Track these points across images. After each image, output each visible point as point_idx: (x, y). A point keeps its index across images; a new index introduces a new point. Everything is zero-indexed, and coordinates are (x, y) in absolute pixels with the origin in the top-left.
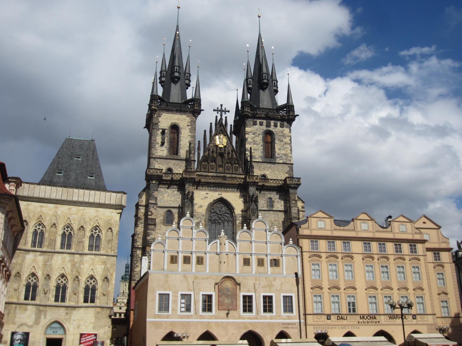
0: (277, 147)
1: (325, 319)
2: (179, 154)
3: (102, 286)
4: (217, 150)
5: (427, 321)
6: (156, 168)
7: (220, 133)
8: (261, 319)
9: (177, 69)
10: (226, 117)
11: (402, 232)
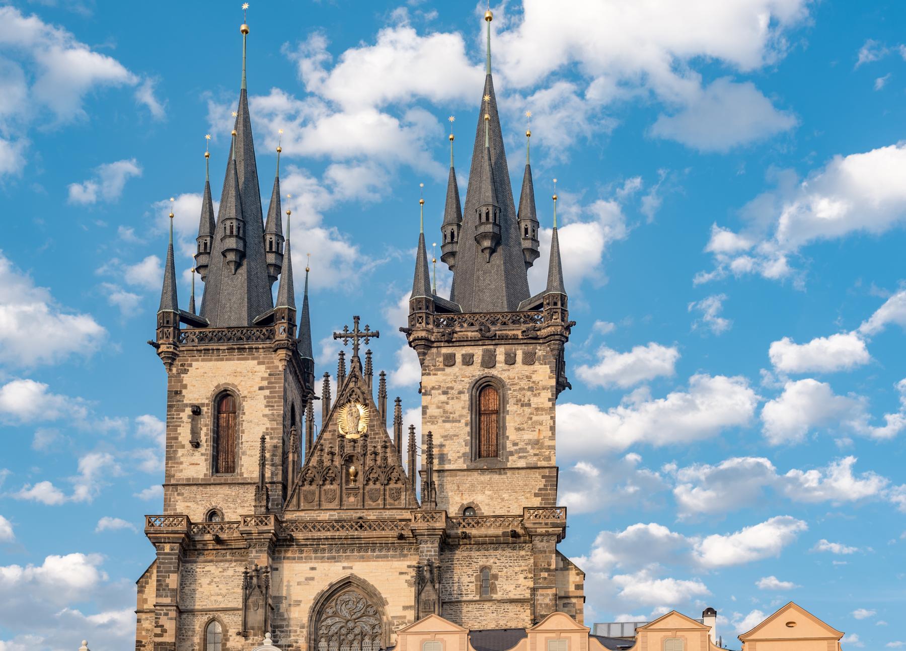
2: (238, 470)
4: (342, 447)
6: (178, 511)
7: (349, 401)
9: (232, 227)
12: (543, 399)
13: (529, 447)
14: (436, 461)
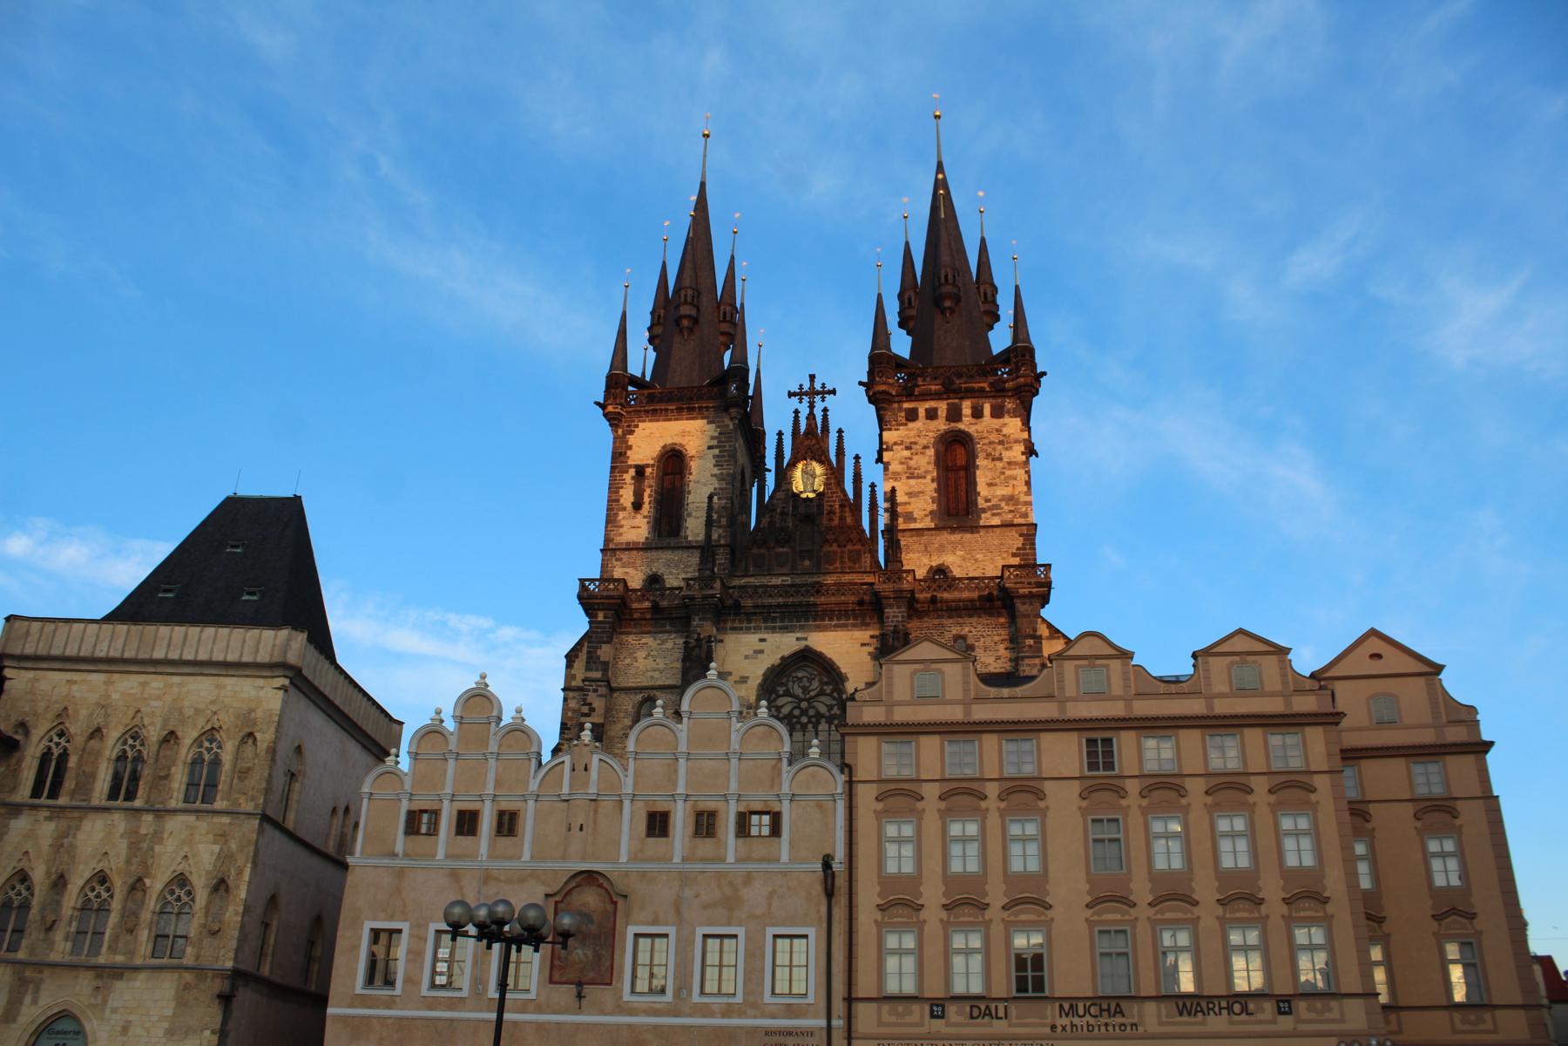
0: (982, 479)
1: (922, 1017)
3: (207, 908)
4: (795, 507)
5: (1342, 1020)
8: (691, 1015)
10: (825, 410)
11: (1242, 692)
12: (1017, 453)
13: (1003, 504)
14: (901, 520)
